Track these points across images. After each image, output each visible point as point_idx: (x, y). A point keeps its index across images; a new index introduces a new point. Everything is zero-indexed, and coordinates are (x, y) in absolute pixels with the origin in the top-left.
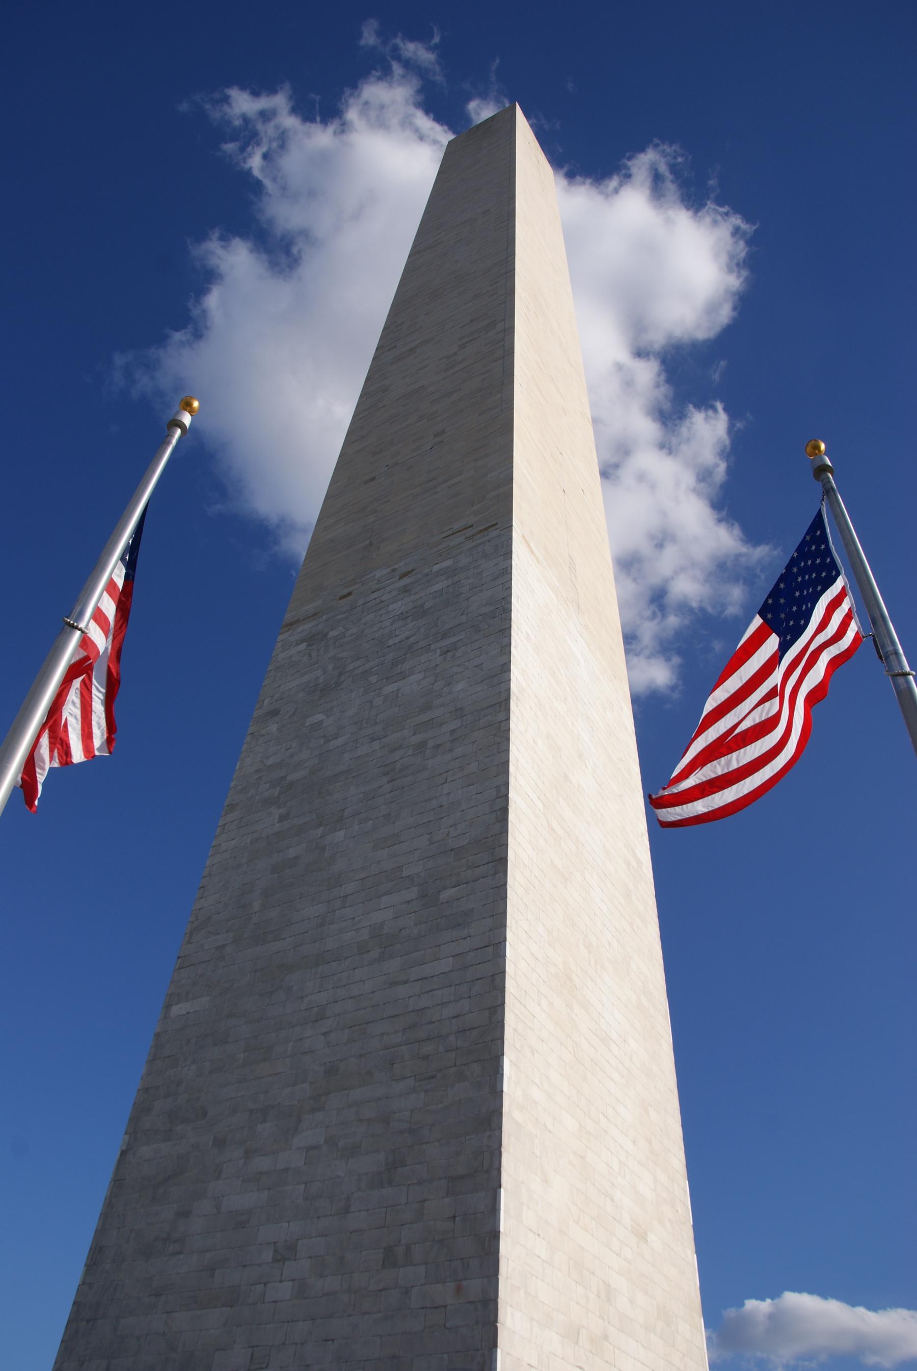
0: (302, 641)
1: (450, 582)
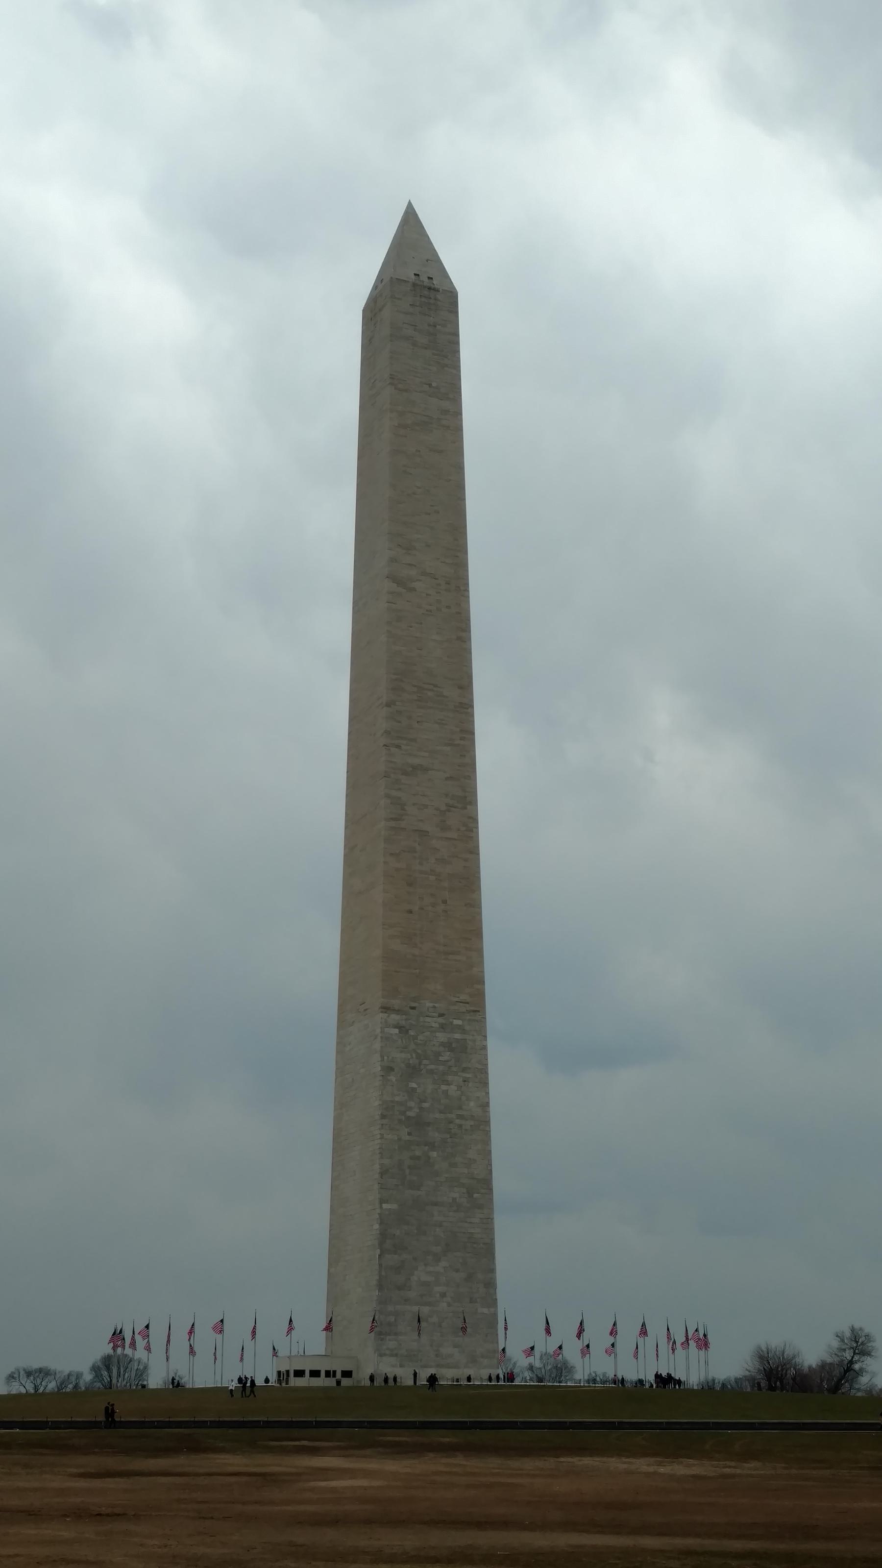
0: (396, 1027)
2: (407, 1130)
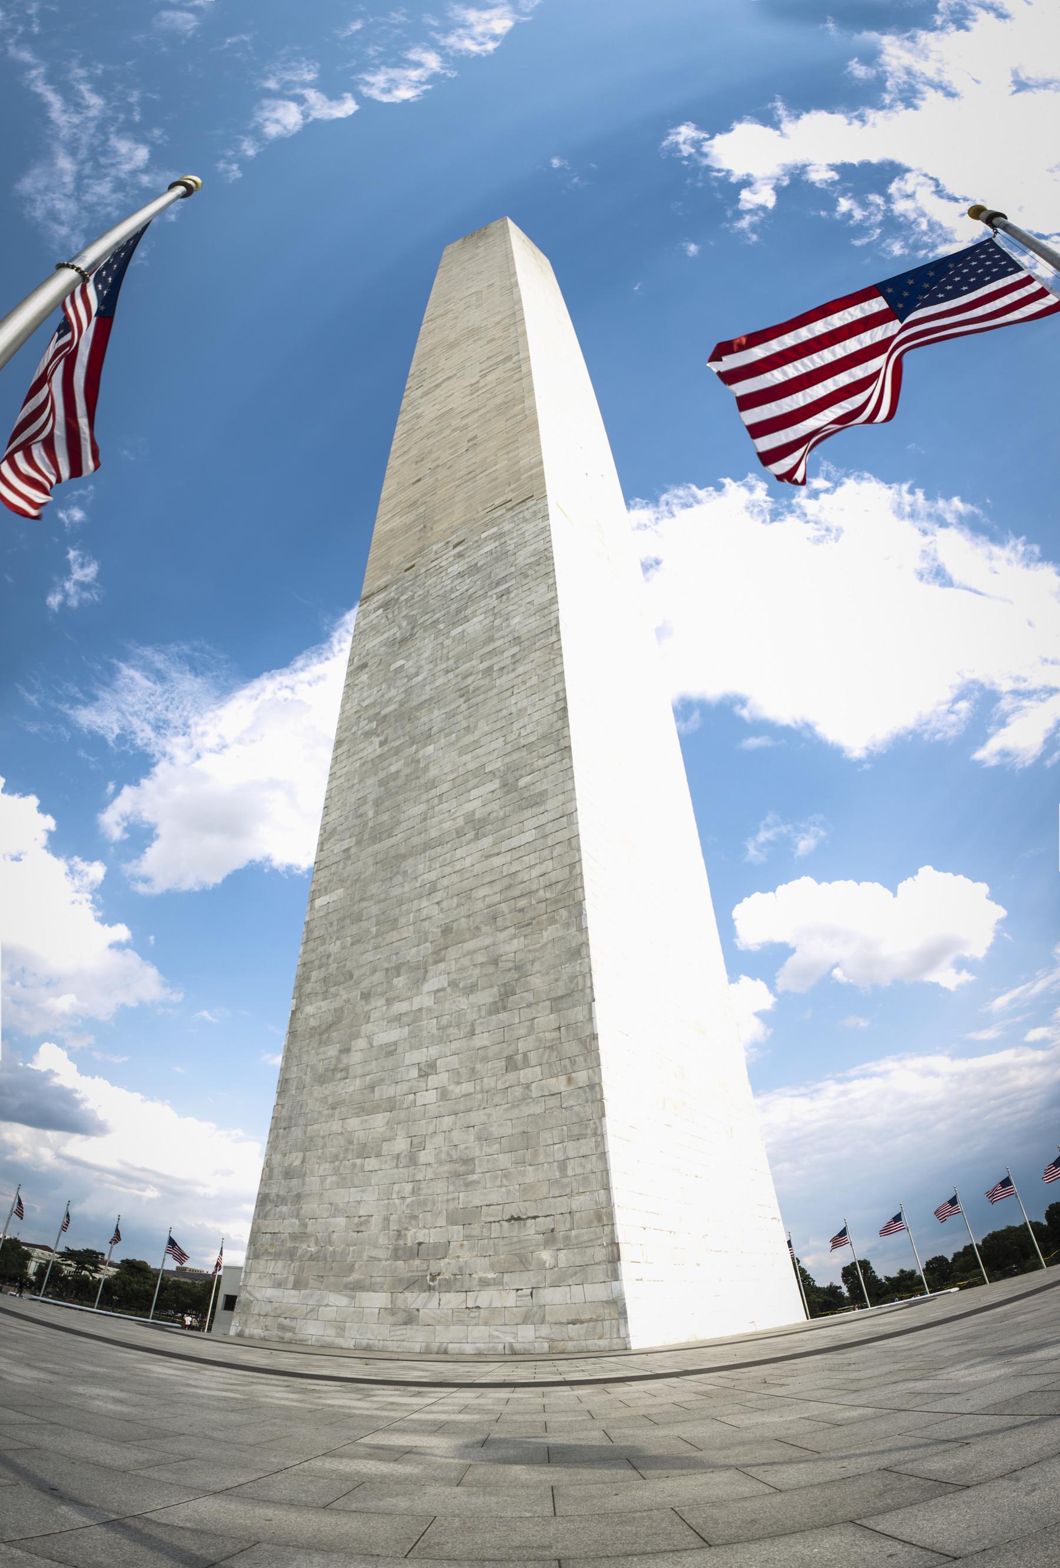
1: (497, 544)
2: (376, 740)
